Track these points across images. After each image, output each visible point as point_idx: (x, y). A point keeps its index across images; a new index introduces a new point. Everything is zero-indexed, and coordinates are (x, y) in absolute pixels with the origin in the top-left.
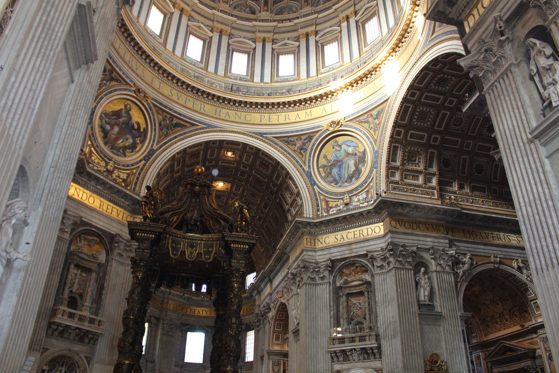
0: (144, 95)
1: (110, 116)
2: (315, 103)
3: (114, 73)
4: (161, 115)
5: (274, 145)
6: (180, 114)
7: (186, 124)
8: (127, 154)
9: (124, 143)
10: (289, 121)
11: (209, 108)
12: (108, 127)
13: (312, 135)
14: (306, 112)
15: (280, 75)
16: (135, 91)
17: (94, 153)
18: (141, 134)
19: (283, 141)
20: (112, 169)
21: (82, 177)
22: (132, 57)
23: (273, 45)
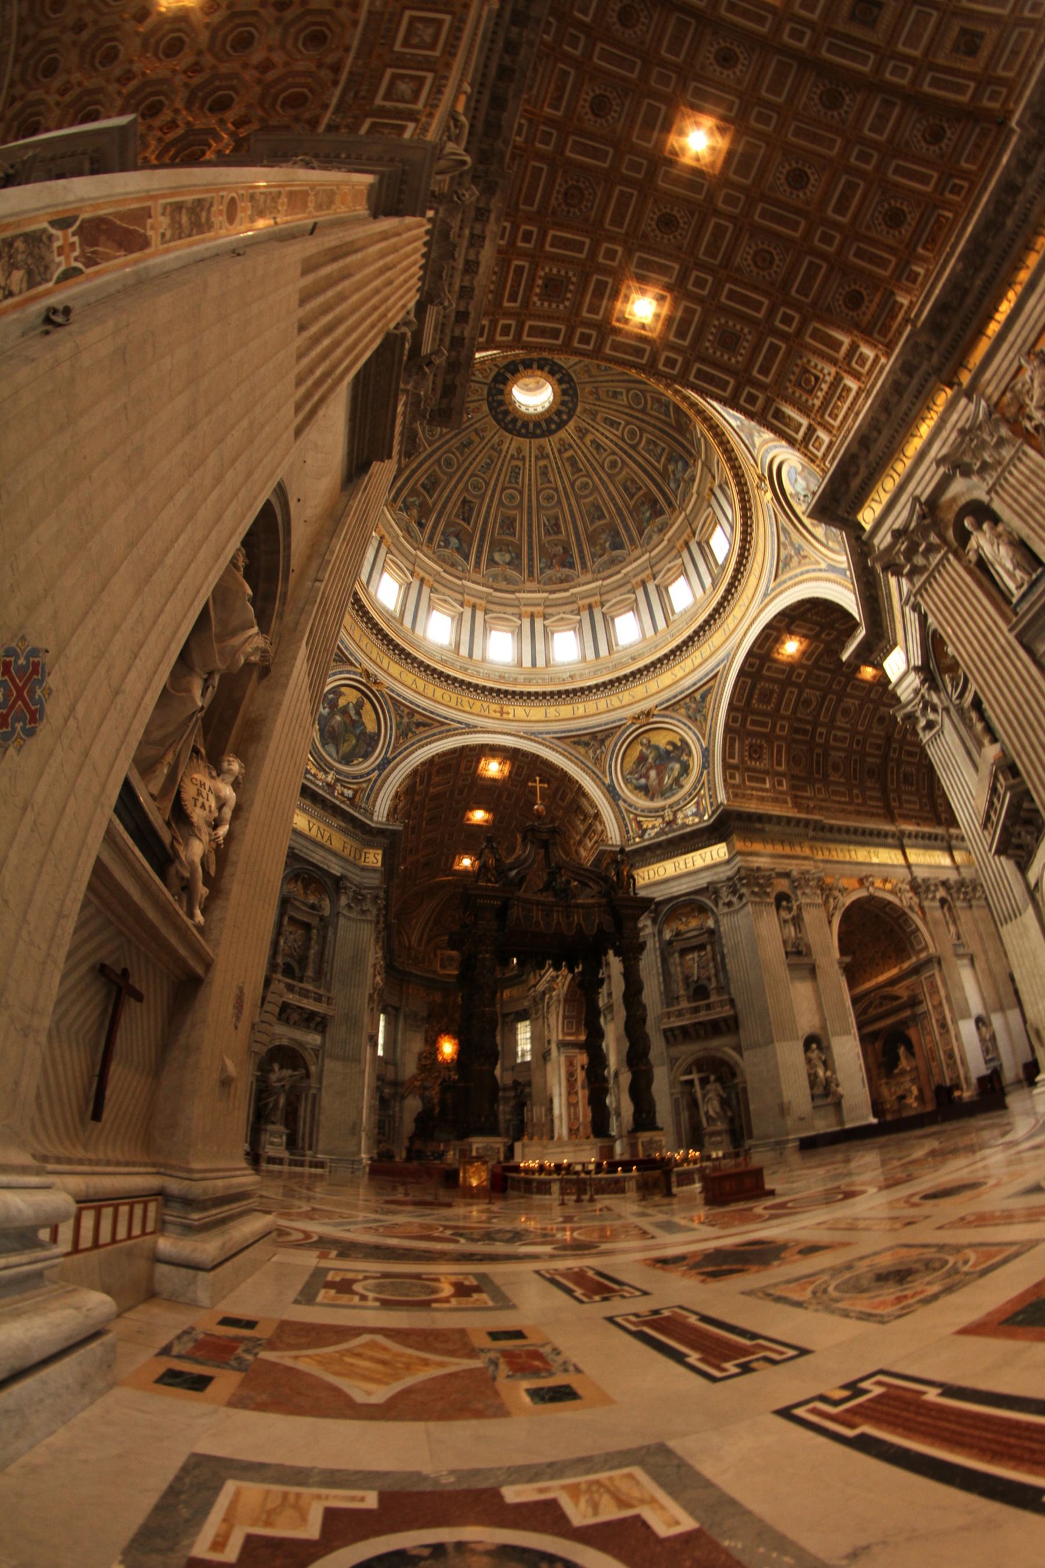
12: (643, 781)
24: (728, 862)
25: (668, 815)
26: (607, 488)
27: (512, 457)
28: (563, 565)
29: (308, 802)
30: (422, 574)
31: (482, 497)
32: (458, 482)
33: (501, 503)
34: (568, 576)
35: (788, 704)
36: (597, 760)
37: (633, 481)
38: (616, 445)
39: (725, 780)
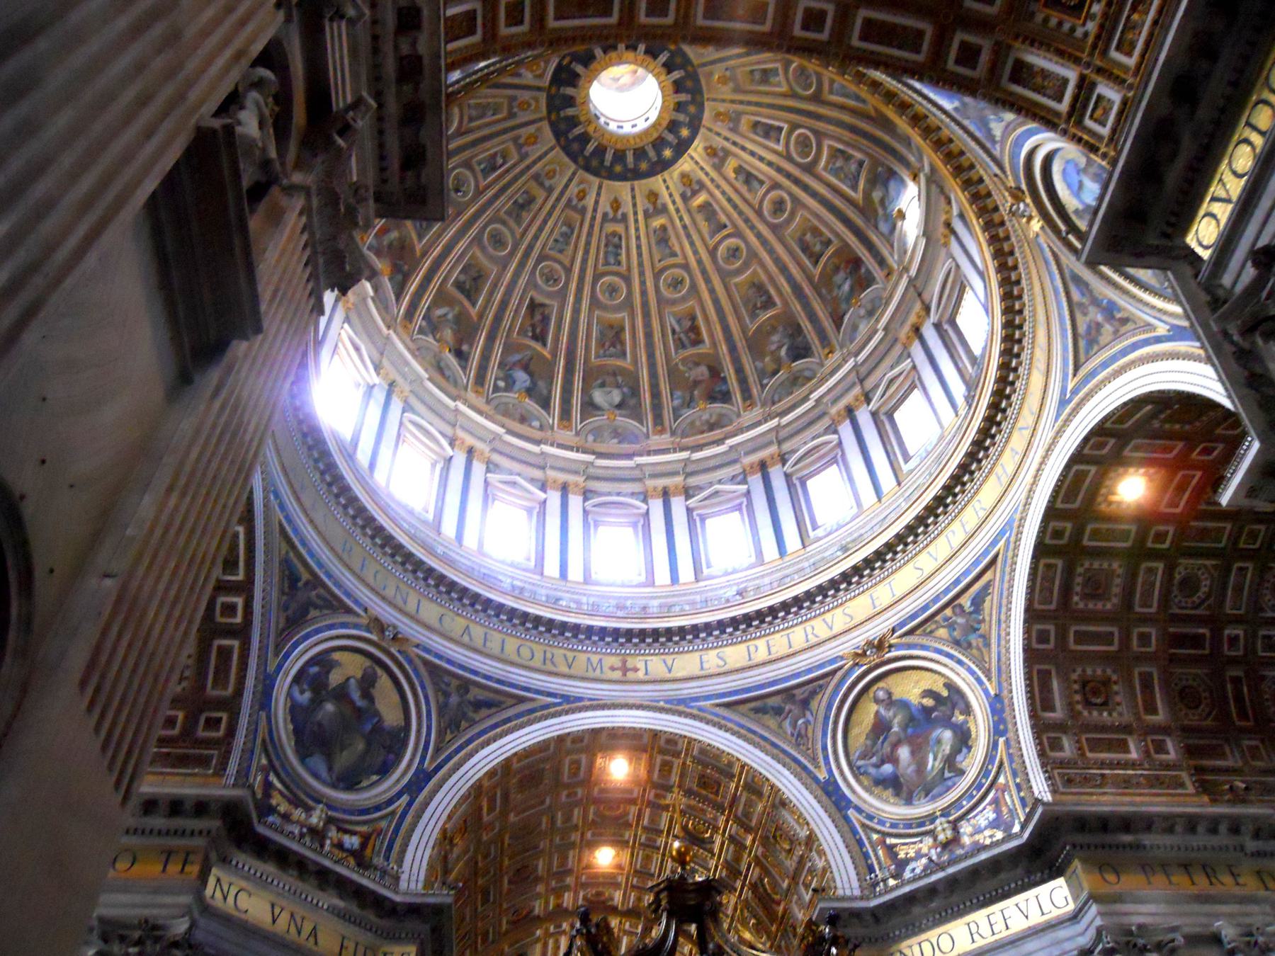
0: (874, 647)
1: (873, 746)
6: (957, 582)
8: (964, 765)
9: (940, 756)
12: (888, 768)
17: (896, 845)
20: (949, 834)
24: (1075, 917)
26: (771, 251)
27: (605, 215)
28: (712, 398)
29: (270, 869)
30: (470, 440)
31: (562, 295)
32: (517, 274)
33: (595, 303)
34: (721, 416)
35: (1147, 594)
36: (800, 738)
37: (816, 232)
38: (779, 170)
39: (1042, 754)
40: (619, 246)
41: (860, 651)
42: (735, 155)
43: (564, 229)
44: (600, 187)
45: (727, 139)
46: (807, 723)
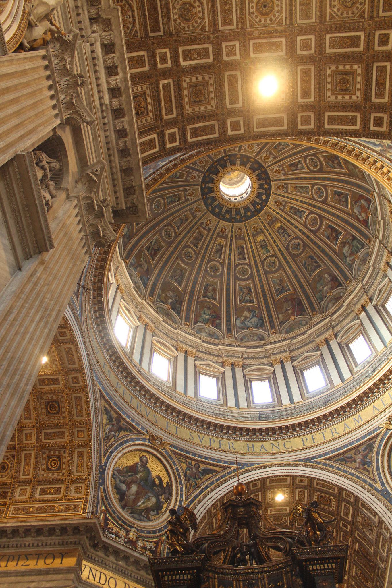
0: (161, 442)
2: (361, 405)
3: (122, 421)
4: (184, 463)
5: (329, 468)
6: (207, 458)
7: (216, 469)
8: (152, 518)
9: (145, 504)
10: (337, 435)
11: (239, 445)
12: (124, 487)
13: (371, 442)
14: (354, 419)
15: (310, 390)
16: (149, 439)
17: (110, 520)
18: (165, 490)
19: (338, 460)
20: (135, 538)
21: (98, 551)
22: (140, 402)
23: (292, 362)
25: (132, 535)
26: (198, 273)
27: (186, 191)
36: (107, 438)
37: (214, 290)
38: (229, 264)
40: (175, 202)
41: (156, 438)
42: (226, 242)
43: (179, 174)
44: (197, 185)
45: (232, 236)
46: (114, 436)
